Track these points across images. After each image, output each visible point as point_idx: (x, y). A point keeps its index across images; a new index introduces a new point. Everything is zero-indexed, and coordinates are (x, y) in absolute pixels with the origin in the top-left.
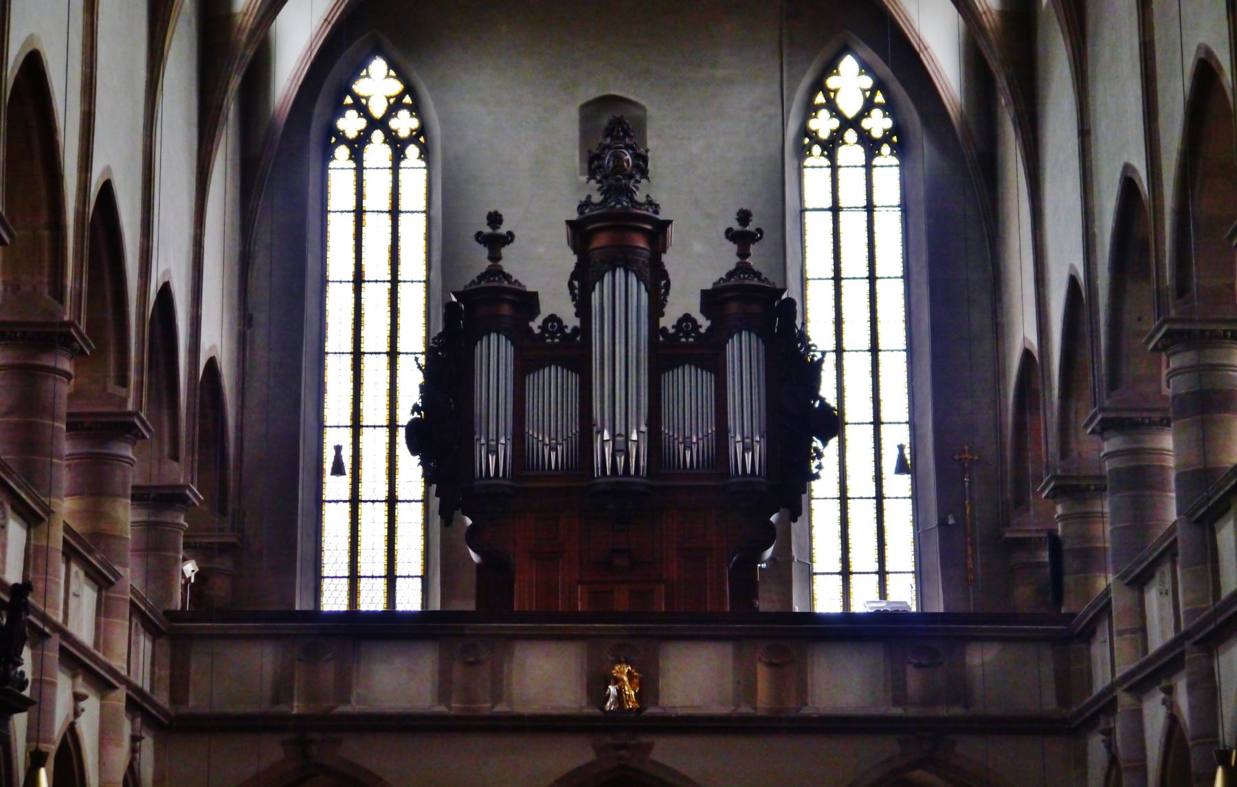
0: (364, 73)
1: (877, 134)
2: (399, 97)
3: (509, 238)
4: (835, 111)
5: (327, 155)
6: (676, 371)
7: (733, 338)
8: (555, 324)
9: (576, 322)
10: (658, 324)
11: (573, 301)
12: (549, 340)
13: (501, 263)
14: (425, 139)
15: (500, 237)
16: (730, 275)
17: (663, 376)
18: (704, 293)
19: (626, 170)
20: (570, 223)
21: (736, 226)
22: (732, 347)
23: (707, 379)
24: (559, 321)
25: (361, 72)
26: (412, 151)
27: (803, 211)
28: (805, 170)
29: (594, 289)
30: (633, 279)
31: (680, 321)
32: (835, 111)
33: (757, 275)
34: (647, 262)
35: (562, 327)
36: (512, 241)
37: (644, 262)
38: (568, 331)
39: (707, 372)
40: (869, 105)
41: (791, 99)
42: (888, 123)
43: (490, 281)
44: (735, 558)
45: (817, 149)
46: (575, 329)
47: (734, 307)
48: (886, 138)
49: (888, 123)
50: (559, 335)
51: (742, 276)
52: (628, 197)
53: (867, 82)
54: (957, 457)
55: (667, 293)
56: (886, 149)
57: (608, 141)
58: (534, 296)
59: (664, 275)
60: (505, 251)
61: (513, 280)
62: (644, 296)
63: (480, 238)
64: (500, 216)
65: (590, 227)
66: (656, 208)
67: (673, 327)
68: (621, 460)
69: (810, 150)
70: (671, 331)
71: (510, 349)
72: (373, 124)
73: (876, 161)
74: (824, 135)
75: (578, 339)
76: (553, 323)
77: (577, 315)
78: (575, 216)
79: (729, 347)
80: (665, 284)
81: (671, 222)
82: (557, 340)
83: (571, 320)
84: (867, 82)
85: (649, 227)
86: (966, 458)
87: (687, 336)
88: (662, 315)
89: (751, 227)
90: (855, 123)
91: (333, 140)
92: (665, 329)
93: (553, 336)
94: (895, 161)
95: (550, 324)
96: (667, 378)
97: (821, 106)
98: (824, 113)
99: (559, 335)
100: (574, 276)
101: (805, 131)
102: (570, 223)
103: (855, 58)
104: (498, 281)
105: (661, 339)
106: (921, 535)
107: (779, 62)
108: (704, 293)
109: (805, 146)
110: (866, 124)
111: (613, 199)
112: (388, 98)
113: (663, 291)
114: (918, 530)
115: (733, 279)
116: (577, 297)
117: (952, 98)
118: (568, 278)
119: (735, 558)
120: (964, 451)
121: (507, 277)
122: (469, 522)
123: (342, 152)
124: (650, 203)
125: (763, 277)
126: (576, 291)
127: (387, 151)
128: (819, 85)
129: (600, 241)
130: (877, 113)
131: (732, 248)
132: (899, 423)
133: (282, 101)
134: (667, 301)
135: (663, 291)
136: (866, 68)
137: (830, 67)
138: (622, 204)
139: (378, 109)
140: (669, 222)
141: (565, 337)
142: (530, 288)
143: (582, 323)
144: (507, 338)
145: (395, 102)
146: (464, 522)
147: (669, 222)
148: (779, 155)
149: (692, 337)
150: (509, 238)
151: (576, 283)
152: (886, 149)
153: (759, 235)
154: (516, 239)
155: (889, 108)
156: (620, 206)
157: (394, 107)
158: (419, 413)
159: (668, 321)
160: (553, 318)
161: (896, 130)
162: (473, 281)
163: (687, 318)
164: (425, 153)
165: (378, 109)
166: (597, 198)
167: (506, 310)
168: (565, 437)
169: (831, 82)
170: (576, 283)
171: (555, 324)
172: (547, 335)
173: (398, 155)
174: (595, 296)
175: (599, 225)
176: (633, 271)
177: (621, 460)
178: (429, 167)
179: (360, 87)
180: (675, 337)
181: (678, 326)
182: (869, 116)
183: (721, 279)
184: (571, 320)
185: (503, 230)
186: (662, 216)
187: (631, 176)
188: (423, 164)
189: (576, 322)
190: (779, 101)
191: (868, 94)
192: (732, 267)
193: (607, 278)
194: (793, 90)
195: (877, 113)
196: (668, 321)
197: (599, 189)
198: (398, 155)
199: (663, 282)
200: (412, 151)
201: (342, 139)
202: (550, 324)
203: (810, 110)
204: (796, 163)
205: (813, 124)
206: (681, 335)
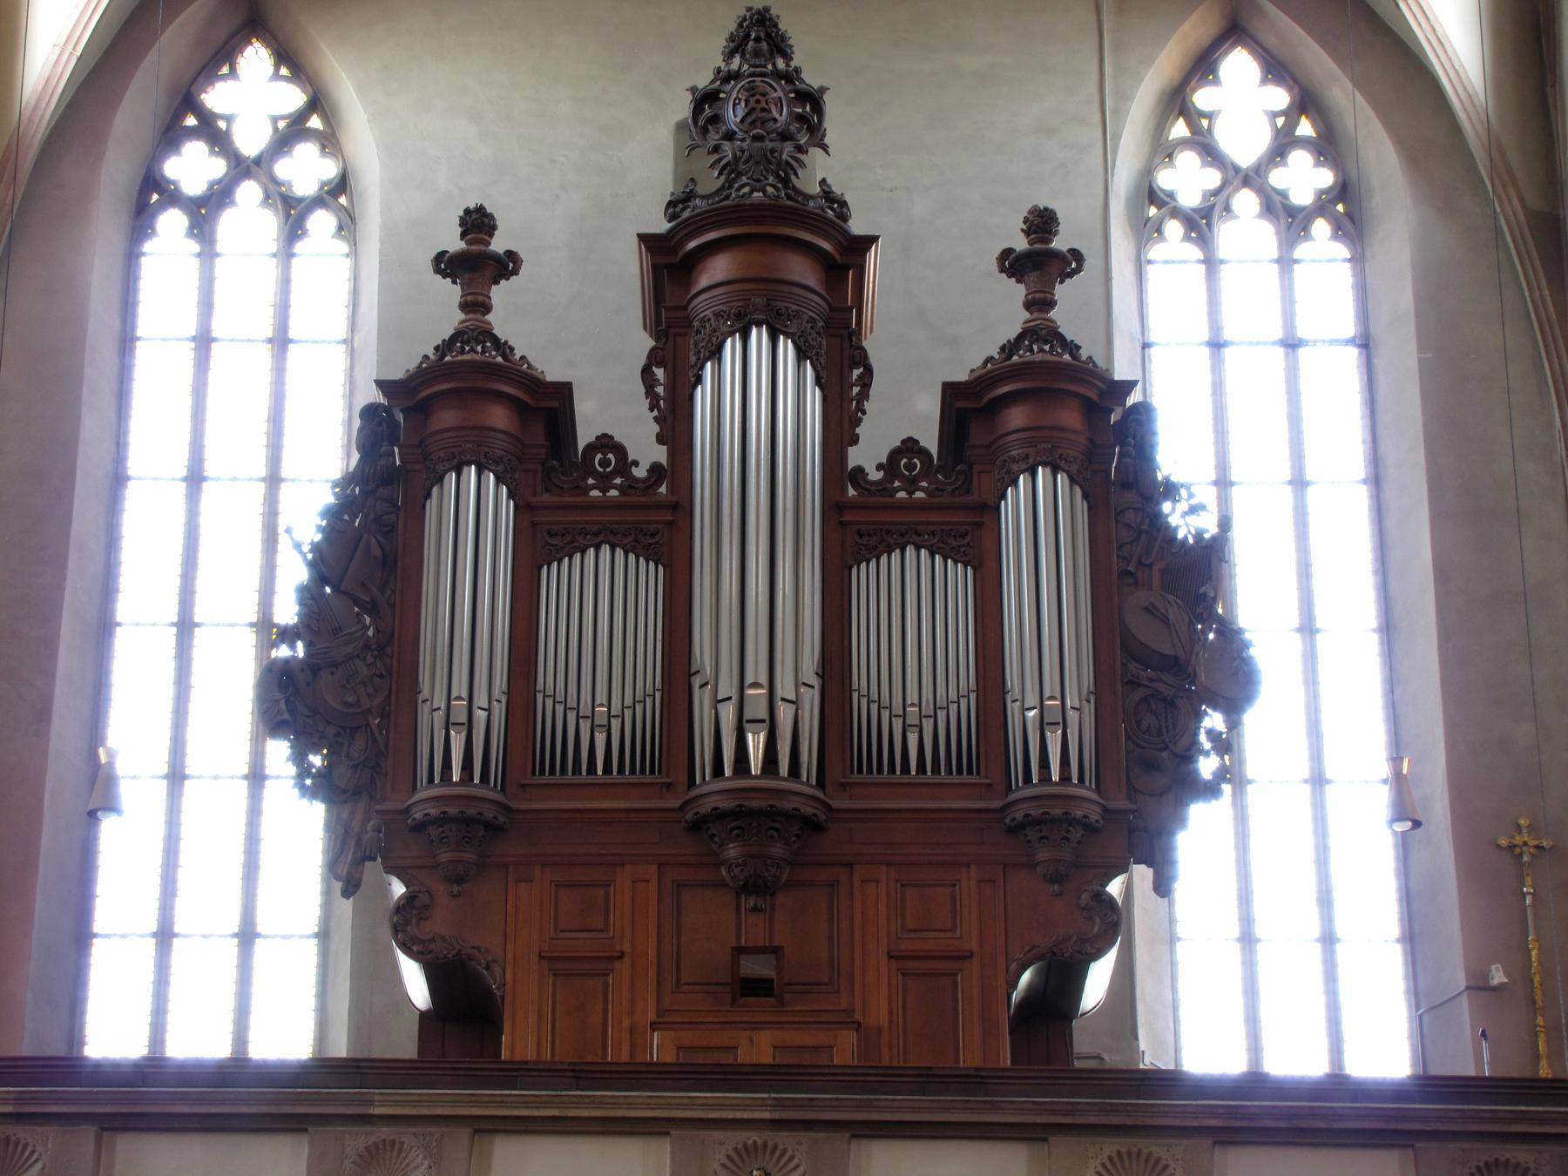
0: (225, 70)
1: (1302, 196)
2: (299, 119)
3: (507, 265)
4: (1210, 153)
5: (140, 220)
6: (884, 558)
7: (1015, 483)
8: (611, 456)
9: (660, 454)
10: (843, 458)
11: (651, 410)
12: (595, 493)
13: (489, 317)
14: (351, 201)
15: (495, 257)
16: (1009, 349)
17: (854, 571)
18: (951, 391)
19: (776, 120)
20: (645, 239)
21: (1021, 244)
22: (1015, 505)
23: (959, 577)
24: (620, 450)
25: (220, 68)
26: (322, 222)
27: (1146, 346)
28: (1150, 268)
29: (699, 380)
30: (786, 349)
31: (895, 455)
32: (1210, 153)
33: (1073, 349)
34: (821, 324)
35: (625, 464)
36: (515, 272)
37: (812, 321)
38: (640, 472)
39: (956, 562)
40: (1283, 145)
41: (1121, 113)
42: (1326, 178)
43: (462, 352)
44: (1026, 977)
45: (1174, 228)
46: (655, 469)
47: (1017, 417)
48: (1322, 206)
49: (1326, 178)
50: (618, 481)
51: (1035, 348)
52: (778, 176)
53: (1280, 98)
54: (1503, 842)
55: (864, 395)
56: (1321, 227)
57: (736, 63)
58: (564, 391)
59: (862, 359)
60: (500, 293)
61: (517, 357)
62: (814, 397)
63: (446, 265)
64: (491, 217)
65: (692, 245)
66: (840, 206)
67: (879, 467)
68: (756, 744)
69: (1159, 230)
70: (875, 475)
71: (507, 508)
72: (242, 168)
73: (1301, 251)
74: (1189, 198)
75: (663, 489)
76: (605, 454)
77: (660, 439)
78: (659, 225)
79: (1007, 508)
80: (860, 377)
81: (874, 239)
82: (613, 493)
83: (646, 450)
84: (1280, 98)
85: (826, 246)
86: (1525, 844)
87: (911, 484)
88: (854, 440)
89: (1059, 244)
90: (1252, 178)
91: (155, 197)
92: (859, 471)
93: (604, 482)
94: (1342, 251)
95: (599, 456)
96: (864, 576)
97: (1184, 143)
98: (1188, 160)
99: (618, 481)
100: (654, 358)
101: (1153, 196)
102: (645, 239)
103: (1253, 52)
104: (483, 352)
105: (851, 492)
106: (1425, 1019)
107: (1095, 25)
108: (951, 391)
109: (1148, 219)
110: (1277, 178)
111: (744, 179)
112: (275, 120)
113: (856, 390)
114: (1418, 1009)
115: (1015, 358)
116: (662, 402)
117: (1470, 96)
118: (642, 360)
119: (1026, 977)
120: (1519, 828)
121: (503, 348)
122: (398, 889)
123: (172, 222)
124: (828, 196)
125: (1084, 354)
126: (660, 390)
127: (269, 223)
128: (1176, 101)
129: (718, 269)
130: (1300, 159)
131: (1016, 291)
132: (1325, 901)
133: (39, 89)
134: (864, 412)
135: (856, 390)
136: (1275, 68)
137: (1203, 66)
138: (764, 192)
139: (251, 139)
140: (872, 240)
141: (632, 485)
142: (553, 374)
143: (672, 455)
144: (498, 480)
145: (289, 126)
146: (386, 890)
147: (872, 240)
148: (1099, 226)
149: (922, 489)
150: (507, 265)
151: (659, 373)
152: (1321, 227)
153: (1074, 265)
154: (524, 269)
155: (1328, 147)
156: (761, 194)
157: (290, 133)
158: (293, 647)
159: (868, 454)
160: (605, 443)
161: (1343, 191)
162: (426, 357)
163: (910, 447)
164: (348, 226)
165: (251, 139)
166: (710, 182)
167: (499, 417)
168: (628, 701)
169: (1203, 98)
170: (659, 373)
171: (611, 456)
172: (591, 481)
173: (294, 229)
174: (703, 397)
175: (712, 236)
176: (787, 335)
177: (756, 744)
178: (354, 253)
179: (216, 98)
180: (883, 488)
181: (890, 466)
182: (1284, 163)
183: (989, 360)
184: (646, 450)
185: (498, 245)
186: (857, 226)
187: (785, 136)
188: (343, 247)
189: (660, 454)
190: (1097, 118)
191: (1280, 121)
192: (1012, 331)
193: (732, 348)
194: (1125, 97)
195: (1300, 159)
196: (868, 454)
197: (712, 166)
198: (294, 229)
199: (856, 373)
200: (322, 222)
201: (172, 197)
202: (599, 456)
203: (1162, 151)
204: (1132, 250)
205: (1165, 179)
206: (897, 484)
